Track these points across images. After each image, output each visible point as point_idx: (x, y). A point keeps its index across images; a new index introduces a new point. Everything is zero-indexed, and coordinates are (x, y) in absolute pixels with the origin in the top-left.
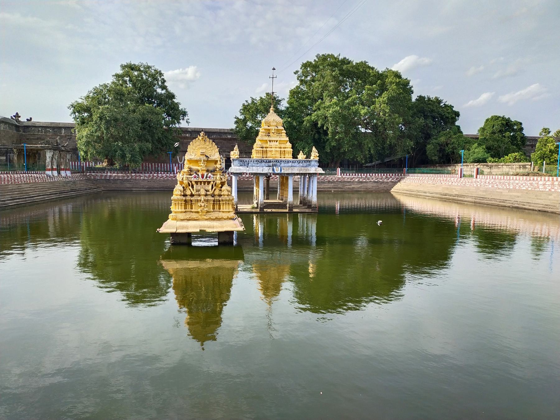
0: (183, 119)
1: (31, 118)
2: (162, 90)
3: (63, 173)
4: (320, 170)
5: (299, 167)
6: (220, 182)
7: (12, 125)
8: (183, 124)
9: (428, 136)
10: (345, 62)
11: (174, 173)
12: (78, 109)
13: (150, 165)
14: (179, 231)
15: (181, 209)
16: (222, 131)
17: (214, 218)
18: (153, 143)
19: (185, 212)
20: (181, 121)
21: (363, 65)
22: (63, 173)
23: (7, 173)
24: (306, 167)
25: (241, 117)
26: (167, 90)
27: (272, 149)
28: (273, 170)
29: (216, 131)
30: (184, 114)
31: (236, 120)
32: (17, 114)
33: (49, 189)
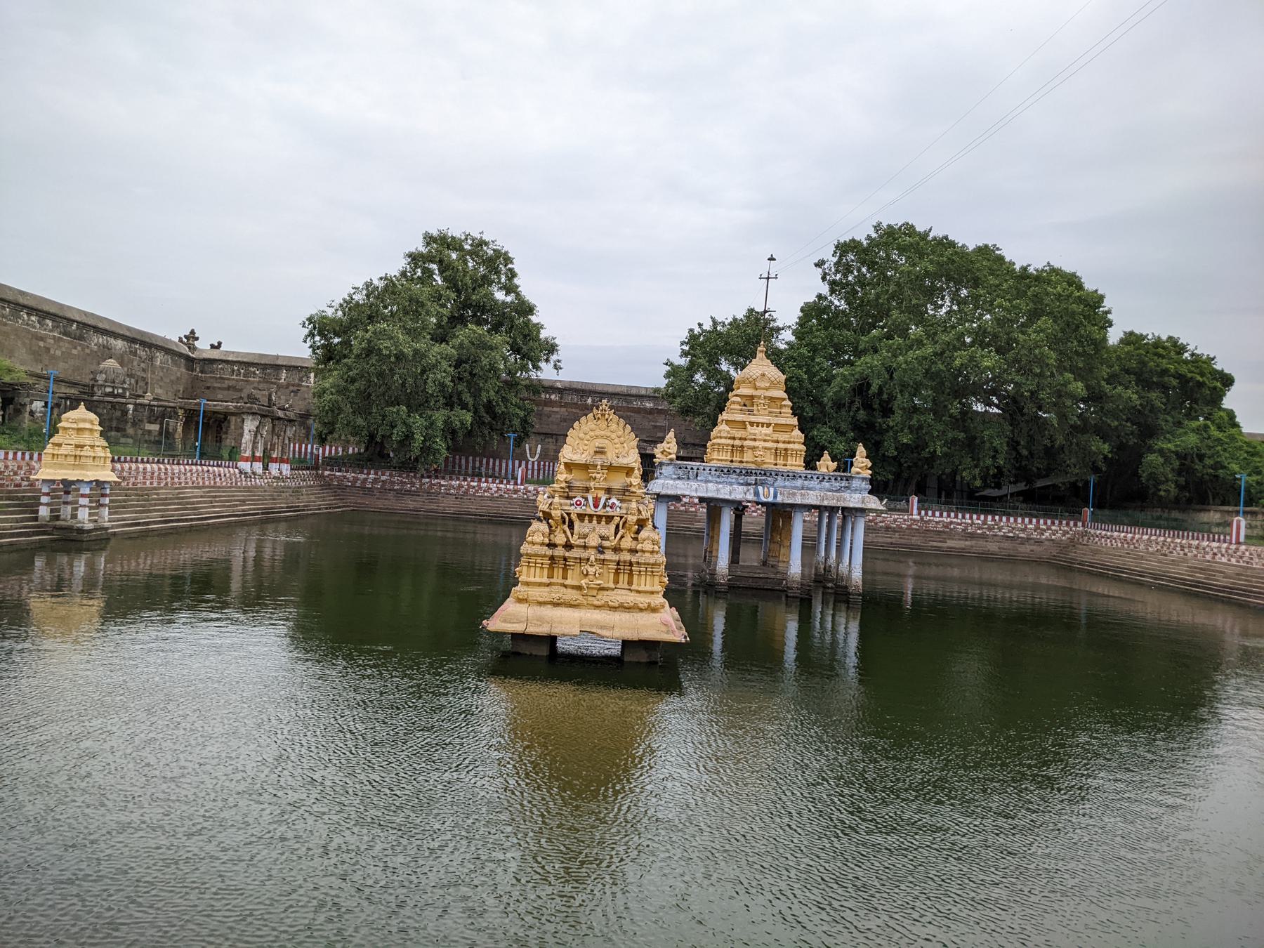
0: (547, 360)
1: (220, 344)
3: (274, 467)
4: (873, 503)
5: (820, 489)
6: (635, 518)
7: (180, 355)
8: (546, 373)
9: (1149, 432)
11: (516, 484)
12: (319, 326)
13: (463, 462)
14: (532, 630)
16: (634, 392)
19: (548, 585)
20: (542, 365)
22: (274, 467)
23: (158, 462)
24: (838, 491)
25: (683, 362)
26: (518, 295)
27: (756, 444)
28: (757, 494)
29: (618, 390)
30: (551, 348)
32: (193, 332)
33: (243, 502)
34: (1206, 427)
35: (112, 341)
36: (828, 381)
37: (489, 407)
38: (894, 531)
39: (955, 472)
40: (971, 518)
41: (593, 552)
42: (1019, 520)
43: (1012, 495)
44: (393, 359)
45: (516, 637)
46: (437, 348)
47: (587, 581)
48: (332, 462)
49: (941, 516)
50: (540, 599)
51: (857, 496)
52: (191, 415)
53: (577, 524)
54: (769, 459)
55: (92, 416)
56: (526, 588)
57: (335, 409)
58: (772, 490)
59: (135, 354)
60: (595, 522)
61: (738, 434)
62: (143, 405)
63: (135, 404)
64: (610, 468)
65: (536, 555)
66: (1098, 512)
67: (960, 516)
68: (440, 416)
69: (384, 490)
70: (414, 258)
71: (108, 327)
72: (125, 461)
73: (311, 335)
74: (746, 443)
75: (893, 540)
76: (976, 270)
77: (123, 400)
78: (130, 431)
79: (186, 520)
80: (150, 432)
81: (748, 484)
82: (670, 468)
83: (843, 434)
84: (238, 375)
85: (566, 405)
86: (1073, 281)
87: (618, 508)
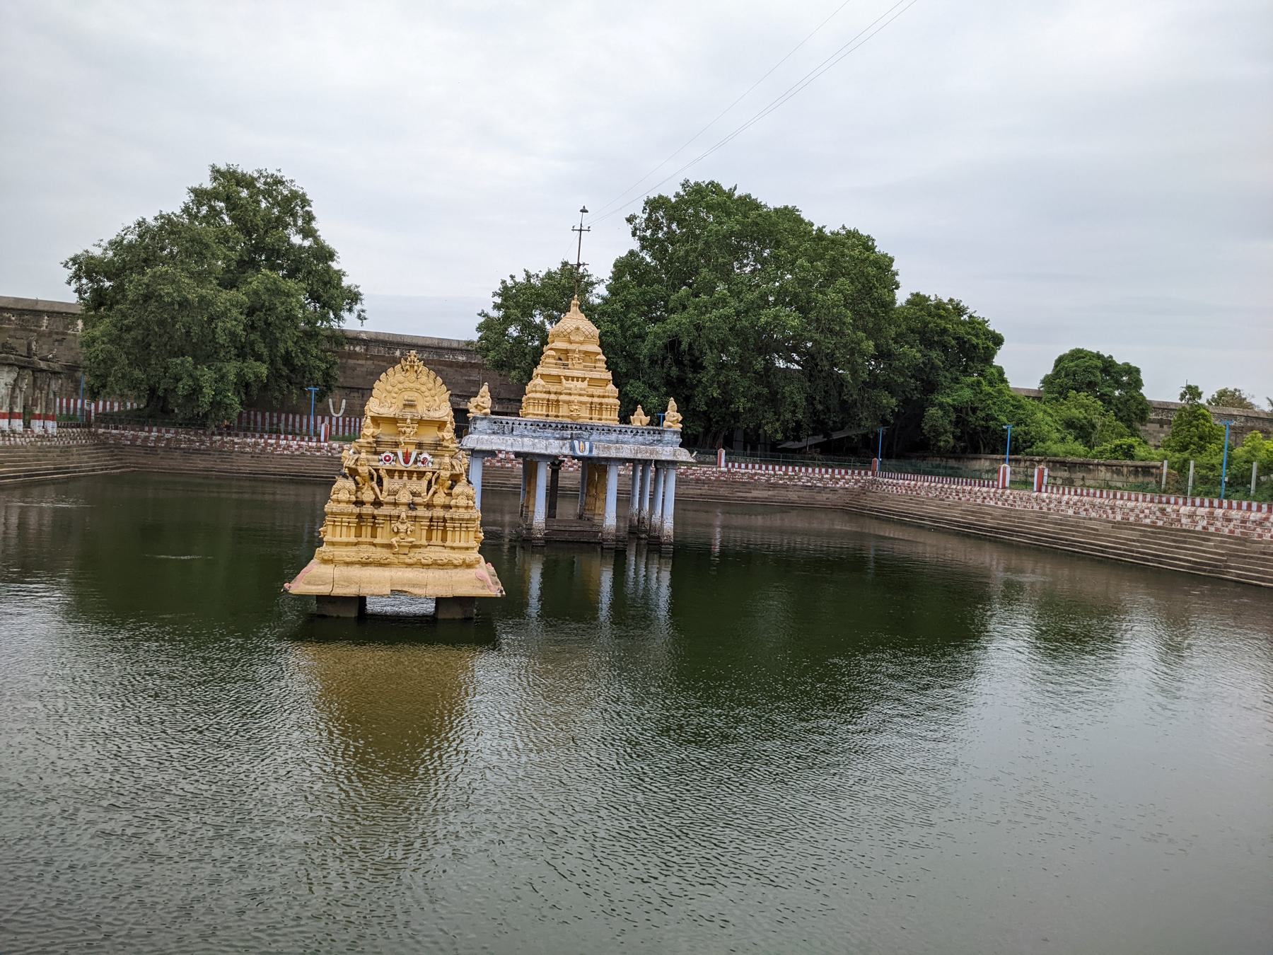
0: (350, 310)
2: (305, 237)
3: (37, 426)
4: (684, 455)
5: (634, 443)
6: (448, 474)
8: (349, 323)
9: (930, 387)
10: (748, 204)
11: (319, 441)
12: (85, 268)
13: (259, 418)
14: (339, 591)
16: (445, 344)
17: (430, 562)
18: (272, 363)
19: (356, 544)
20: (345, 314)
21: (789, 215)
22: (37, 426)
25: (495, 314)
26: (316, 239)
28: (572, 448)
30: (354, 297)
31: (482, 320)
34: (979, 383)
36: (642, 337)
37: (287, 359)
38: (704, 483)
39: (759, 426)
41: (404, 508)
42: (817, 470)
44: (176, 307)
45: (321, 599)
46: (226, 295)
47: (397, 538)
48: (106, 419)
49: (747, 467)
50: (348, 560)
51: (669, 449)
53: (386, 481)
54: (585, 413)
56: (331, 548)
57: (109, 360)
58: (587, 444)
60: (405, 478)
61: (553, 388)
64: (421, 422)
65: (342, 514)
68: (231, 369)
69: (168, 448)
70: (200, 195)
73: (77, 276)
74: (562, 397)
75: (703, 492)
76: (777, 231)
82: (485, 422)
83: (656, 389)
85: (373, 358)
86: (866, 244)
87: (430, 463)
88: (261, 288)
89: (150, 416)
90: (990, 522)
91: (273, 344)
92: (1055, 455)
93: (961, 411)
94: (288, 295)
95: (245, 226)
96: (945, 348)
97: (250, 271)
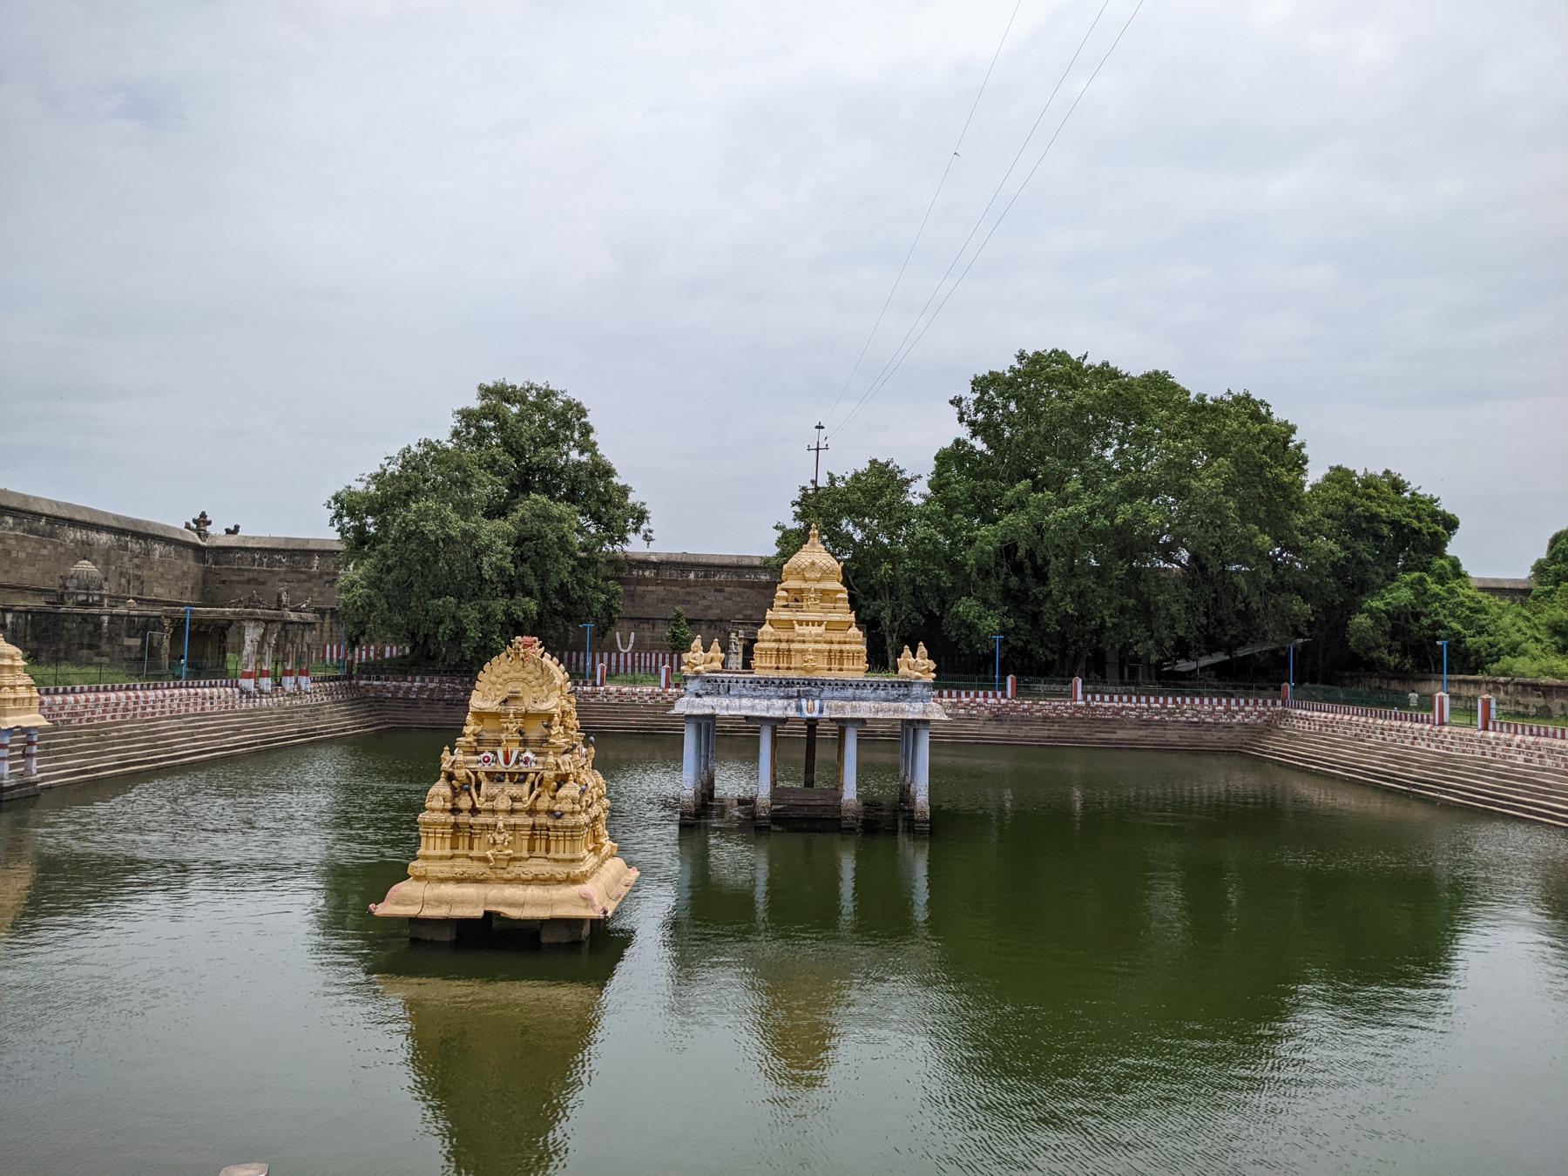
0: (636, 530)
1: (237, 528)
2: (581, 453)
3: (289, 683)
5: (875, 700)
6: (552, 774)
8: (635, 546)
11: (594, 684)
12: (346, 505)
15: (443, 848)
16: (746, 562)
18: (545, 597)
19: (452, 857)
20: (631, 536)
22: (289, 683)
23: (128, 688)
24: (895, 700)
25: (798, 525)
28: (799, 708)
29: (727, 561)
31: (780, 534)
32: (203, 515)
33: (238, 731)
34: (1422, 581)
35: (94, 535)
36: (970, 542)
38: (1054, 721)
40: (1148, 701)
42: (1206, 701)
43: (1203, 669)
45: (414, 921)
48: (369, 669)
49: (1111, 700)
51: (919, 705)
52: (178, 625)
55: (13, 649)
58: (817, 703)
59: (126, 548)
61: (784, 635)
62: (120, 616)
63: (111, 615)
65: (435, 824)
66: (1300, 691)
67: (1134, 699)
68: (498, 606)
69: (431, 701)
70: (466, 415)
71: (88, 519)
72: (82, 691)
73: (339, 516)
75: (1052, 733)
76: (1143, 400)
77: (96, 611)
78: (105, 648)
79: (154, 761)
80: (129, 648)
81: (789, 697)
82: (697, 682)
84: (260, 564)
87: (533, 762)
88: (528, 514)
89: (414, 664)
90: (1416, 773)
91: (543, 577)
92: (1523, 675)
93: (1398, 618)
94: (560, 520)
95: (510, 447)
96: (1378, 537)
97: (521, 496)
